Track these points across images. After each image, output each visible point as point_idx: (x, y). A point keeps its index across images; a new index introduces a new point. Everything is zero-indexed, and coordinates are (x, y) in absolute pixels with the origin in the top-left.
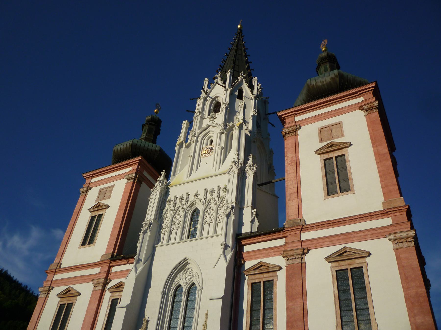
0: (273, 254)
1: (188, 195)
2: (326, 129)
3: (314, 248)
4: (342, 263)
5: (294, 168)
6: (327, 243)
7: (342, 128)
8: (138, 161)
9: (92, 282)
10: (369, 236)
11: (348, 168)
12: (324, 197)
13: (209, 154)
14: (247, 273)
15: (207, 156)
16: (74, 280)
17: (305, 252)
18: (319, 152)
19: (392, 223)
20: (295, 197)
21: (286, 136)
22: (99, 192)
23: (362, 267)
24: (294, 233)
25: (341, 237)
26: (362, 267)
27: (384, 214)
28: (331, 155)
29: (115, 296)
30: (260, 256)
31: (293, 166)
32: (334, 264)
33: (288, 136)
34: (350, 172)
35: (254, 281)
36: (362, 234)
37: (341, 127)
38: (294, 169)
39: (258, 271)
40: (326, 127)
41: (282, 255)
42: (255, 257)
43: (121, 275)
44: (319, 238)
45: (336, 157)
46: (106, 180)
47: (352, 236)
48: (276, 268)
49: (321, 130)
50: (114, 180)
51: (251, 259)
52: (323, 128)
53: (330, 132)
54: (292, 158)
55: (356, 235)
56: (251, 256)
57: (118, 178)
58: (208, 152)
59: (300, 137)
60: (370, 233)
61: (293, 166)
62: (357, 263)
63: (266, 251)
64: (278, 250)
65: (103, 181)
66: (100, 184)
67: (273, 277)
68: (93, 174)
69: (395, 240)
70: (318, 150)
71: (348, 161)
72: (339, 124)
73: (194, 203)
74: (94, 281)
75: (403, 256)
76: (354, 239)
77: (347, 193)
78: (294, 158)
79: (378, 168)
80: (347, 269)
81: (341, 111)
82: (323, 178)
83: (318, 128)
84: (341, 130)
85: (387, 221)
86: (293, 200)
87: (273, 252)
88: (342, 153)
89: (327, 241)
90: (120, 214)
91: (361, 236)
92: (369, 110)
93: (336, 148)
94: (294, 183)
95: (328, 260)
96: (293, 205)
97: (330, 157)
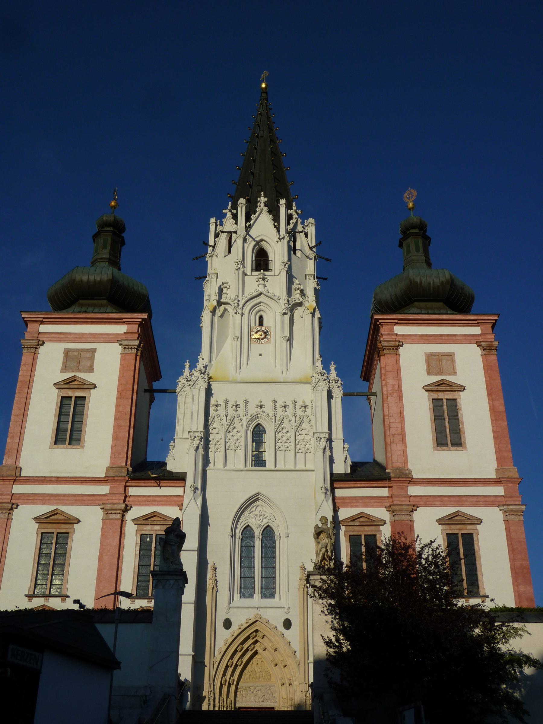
0: (375, 504)
1: (247, 402)
2: (435, 357)
3: (423, 506)
4: (453, 527)
5: (396, 401)
6: (437, 503)
7: (454, 363)
8: (140, 320)
9: (102, 506)
10: (481, 503)
11: (460, 418)
12: (433, 447)
13: (263, 341)
14: (345, 523)
15: (260, 343)
16: (59, 498)
17: (415, 507)
18: (428, 388)
19: (504, 494)
20: (400, 441)
21: (385, 352)
22: (63, 355)
23: (472, 534)
24: (401, 484)
25: (453, 499)
26: (472, 534)
27: (497, 482)
28: (441, 395)
29: (146, 530)
30: (358, 504)
31: (395, 397)
32: (445, 527)
33: (388, 352)
34: (463, 424)
35: (352, 534)
36: (475, 499)
37: (453, 361)
38: (397, 403)
39: (359, 523)
40: (434, 354)
41: (386, 508)
42: (352, 505)
43: (148, 501)
44: (430, 496)
45: (447, 399)
47: (464, 499)
48: (381, 523)
49: (430, 356)
50: (92, 339)
51: (346, 506)
52: (431, 354)
53: (440, 363)
54: (393, 385)
55: (469, 500)
56: (346, 503)
57: (102, 339)
58: (262, 337)
59: (401, 358)
60: (482, 500)
61: (395, 397)
62: (468, 529)
63: (366, 500)
64: (380, 501)
66: (62, 339)
67: (376, 532)
68: (44, 318)
69: (506, 512)
70: (426, 386)
71: (461, 409)
72: (450, 356)
73: (256, 417)
74: (105, 505)
75: (512, 528)
76: (466, 503)
77: (458, 448)
78: (396, 388)
79: (493, 427)
80: (458, 534)
81: (454, 338)
82: (431, 424)
83: (425, 353)
84: (453, 365)
85: (499, 491)
86: (397, 443)
87: (375, 502)
88: (454, 397)
89: (438, 501)
90: (124, 405)
91: (473, 501)
92: (487, 349)
94: (397, 421)
95: (440, 522)
96: (397, 450)
97: (440, 398)
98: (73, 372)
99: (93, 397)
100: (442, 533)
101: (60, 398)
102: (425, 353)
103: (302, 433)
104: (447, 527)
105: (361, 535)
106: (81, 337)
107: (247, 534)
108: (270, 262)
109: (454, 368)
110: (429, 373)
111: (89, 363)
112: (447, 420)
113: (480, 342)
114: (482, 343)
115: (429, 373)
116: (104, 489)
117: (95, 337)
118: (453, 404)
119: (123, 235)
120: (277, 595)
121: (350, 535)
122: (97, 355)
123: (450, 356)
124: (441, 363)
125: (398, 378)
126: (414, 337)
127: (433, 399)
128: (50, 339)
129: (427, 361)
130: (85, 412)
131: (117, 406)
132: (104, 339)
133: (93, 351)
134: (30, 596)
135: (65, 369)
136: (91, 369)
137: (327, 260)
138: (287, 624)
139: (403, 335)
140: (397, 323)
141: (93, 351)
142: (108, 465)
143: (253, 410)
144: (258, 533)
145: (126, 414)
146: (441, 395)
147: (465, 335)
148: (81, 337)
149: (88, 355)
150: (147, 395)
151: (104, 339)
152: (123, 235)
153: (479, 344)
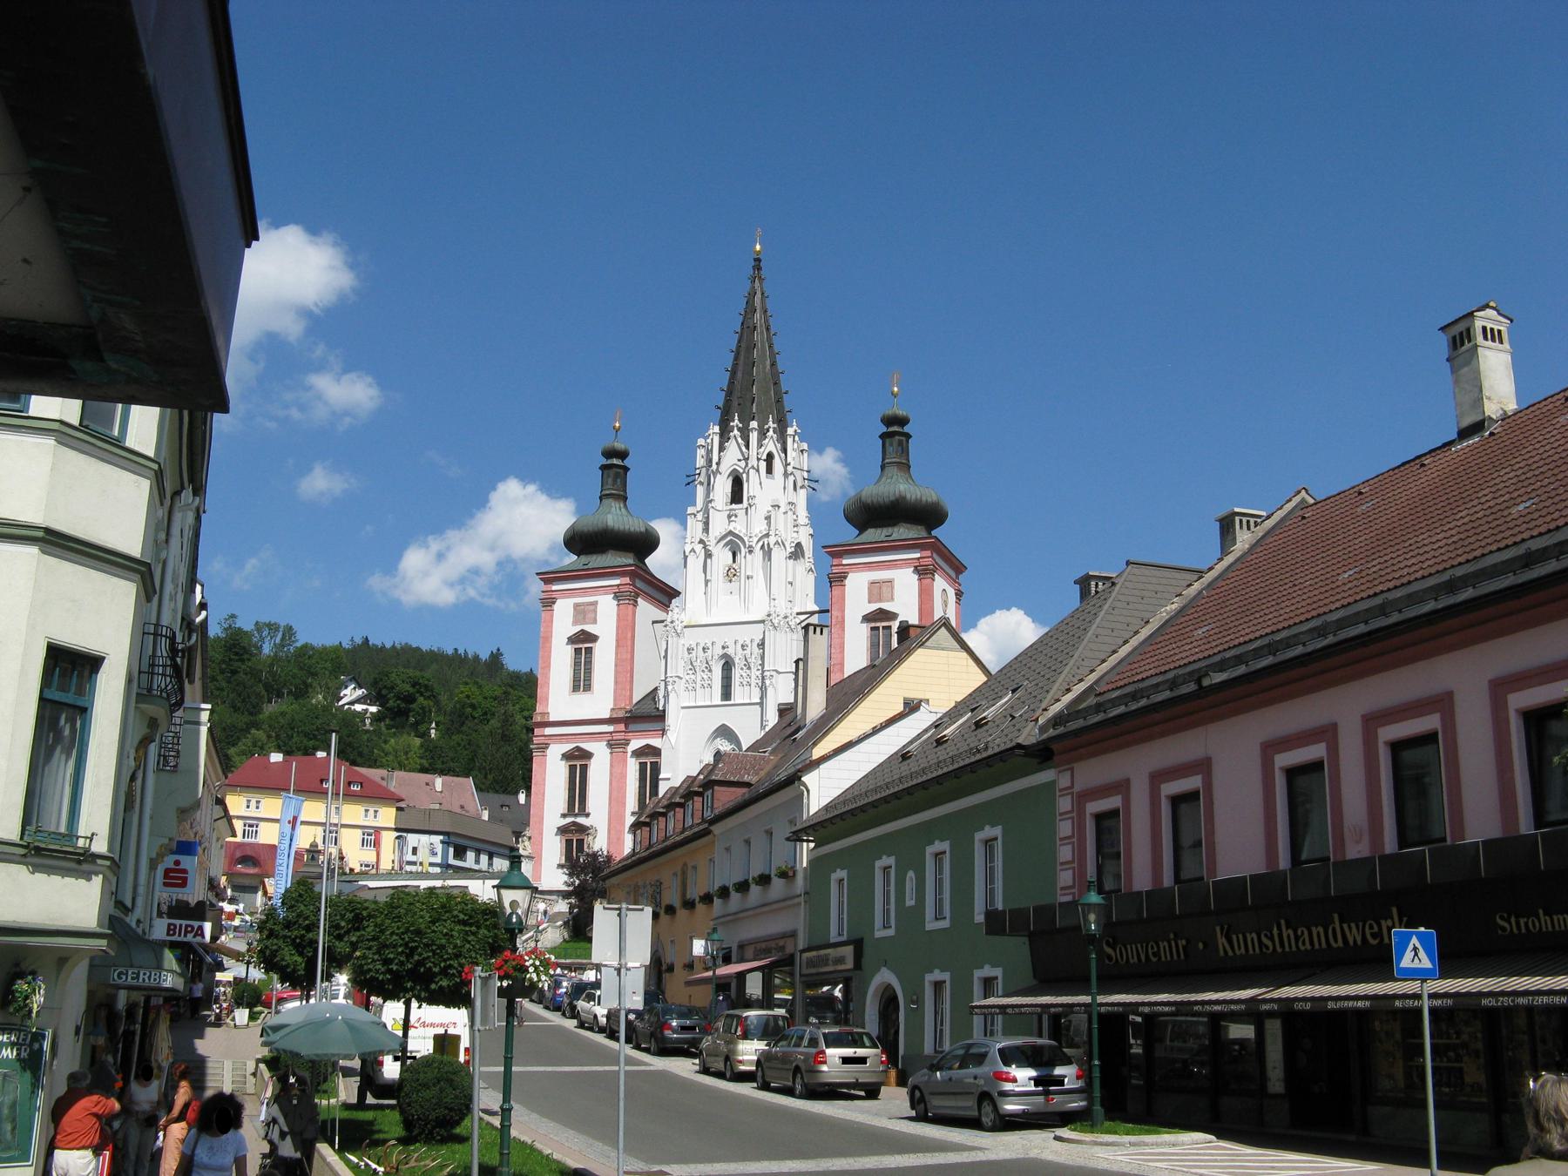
18: (867, 618)
37: (892, 588)
72: (890, 582)
73: (725, 656)
78: (840, 618)
99: (598, 648)
111: (593, 615)
115: (869, 602)
116: (610, 728)
125: (843, 611)
131: (617, 654)
133: (595, 604)
134: (564, 816)
135: (575, 623)
136: (595, 621)
141: (595, 604)
142: (612, 706)
143: (721, 652)
146: (878, 624)
149: (592, 607)
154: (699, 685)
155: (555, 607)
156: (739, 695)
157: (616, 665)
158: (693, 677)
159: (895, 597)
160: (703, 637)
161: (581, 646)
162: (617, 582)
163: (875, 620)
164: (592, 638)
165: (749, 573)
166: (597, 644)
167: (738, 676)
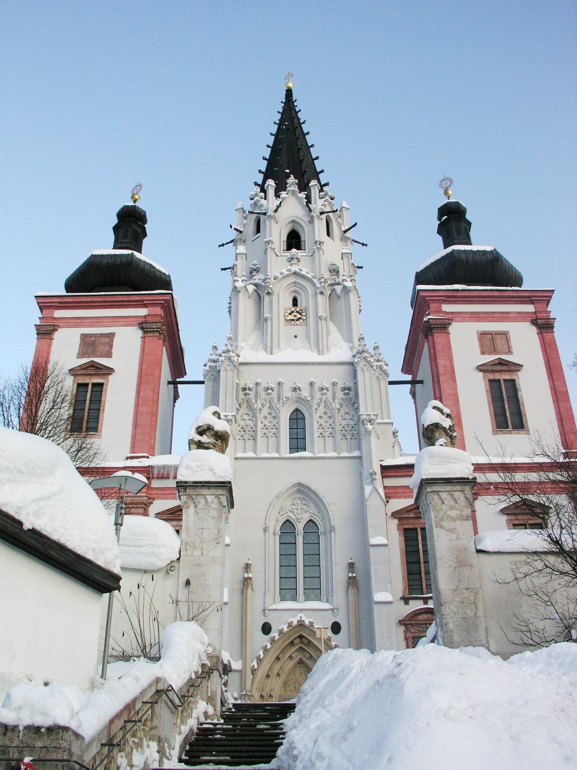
4: (520, 517)
8: (163, 302)
13: (298, 322)
18: (482, 368)
22: (79, 341)
32: (510, 517)
35: (406, 527)
46: (93, 321)
49: (482, 335)
56: (398, 493)
57: (121, 323)
59: (451, 336)
65: (87, 321)
68: (59, 303)
70: (481, 365)
71: (520, 390)
72: (505, 334)
81: (507, 316)
83: (477, 331)
84: (508, 343)
93: (505, 368)
98: (89, 357)
100: (507, 523)
101: (76, 385)
102: (477, 331)
103: (346, 418)
104: (514, 517)
105: (416, 529)
106: (98, 321)
107: (286, 529)
108: (302, 243)
109: (509, 346)
110: (483, 353)
112: (506, 402)
113: (536, 320)
114: (538, 321)
115: (483, 353)
117: (115, 320)
118: (512, 385)
119: (145, 226)
120: (324, 597)
121: (405, 529)
122: (116, 341)
123: (505, 334)
124: (495, 342)
125: (451, 359)
126: (464, 316)
127: (490, 381)
128: (66, 324)
129: (480, 340)
130: (103, 399)
131: (138, 392)
132: (124, 323)
133: (112, 335)
135: (81, 355)
136: (109, 355)
137: (363, 244)
138: (336, 628)
139: (452, 313)
140: (444, 301)
141: (112, 335)
144: (300, 527)
145: (147, 400)
146: (497, 376)
147: (519, 313)
148: (98, 321)
149: (106, 340)
150: (171, 386)
151: (124, 323)
152: (145, 226)
153: (534, 322)
154: (260, 434)
155: (57, 335)
156: (317, 445)
157: (137, 405)
158: (251, 423)
159: (513, 349)
160: (268, 378)
161: (86, 380)
162: (143, 312)
163: (493, 371)
164: (109, 371)
165: (319, 315)
166: (110, 377)
167: (316, 426)
